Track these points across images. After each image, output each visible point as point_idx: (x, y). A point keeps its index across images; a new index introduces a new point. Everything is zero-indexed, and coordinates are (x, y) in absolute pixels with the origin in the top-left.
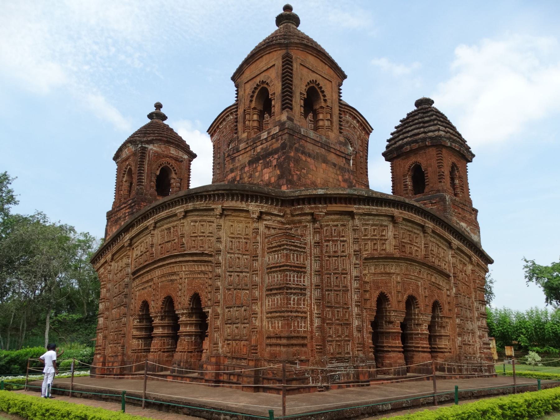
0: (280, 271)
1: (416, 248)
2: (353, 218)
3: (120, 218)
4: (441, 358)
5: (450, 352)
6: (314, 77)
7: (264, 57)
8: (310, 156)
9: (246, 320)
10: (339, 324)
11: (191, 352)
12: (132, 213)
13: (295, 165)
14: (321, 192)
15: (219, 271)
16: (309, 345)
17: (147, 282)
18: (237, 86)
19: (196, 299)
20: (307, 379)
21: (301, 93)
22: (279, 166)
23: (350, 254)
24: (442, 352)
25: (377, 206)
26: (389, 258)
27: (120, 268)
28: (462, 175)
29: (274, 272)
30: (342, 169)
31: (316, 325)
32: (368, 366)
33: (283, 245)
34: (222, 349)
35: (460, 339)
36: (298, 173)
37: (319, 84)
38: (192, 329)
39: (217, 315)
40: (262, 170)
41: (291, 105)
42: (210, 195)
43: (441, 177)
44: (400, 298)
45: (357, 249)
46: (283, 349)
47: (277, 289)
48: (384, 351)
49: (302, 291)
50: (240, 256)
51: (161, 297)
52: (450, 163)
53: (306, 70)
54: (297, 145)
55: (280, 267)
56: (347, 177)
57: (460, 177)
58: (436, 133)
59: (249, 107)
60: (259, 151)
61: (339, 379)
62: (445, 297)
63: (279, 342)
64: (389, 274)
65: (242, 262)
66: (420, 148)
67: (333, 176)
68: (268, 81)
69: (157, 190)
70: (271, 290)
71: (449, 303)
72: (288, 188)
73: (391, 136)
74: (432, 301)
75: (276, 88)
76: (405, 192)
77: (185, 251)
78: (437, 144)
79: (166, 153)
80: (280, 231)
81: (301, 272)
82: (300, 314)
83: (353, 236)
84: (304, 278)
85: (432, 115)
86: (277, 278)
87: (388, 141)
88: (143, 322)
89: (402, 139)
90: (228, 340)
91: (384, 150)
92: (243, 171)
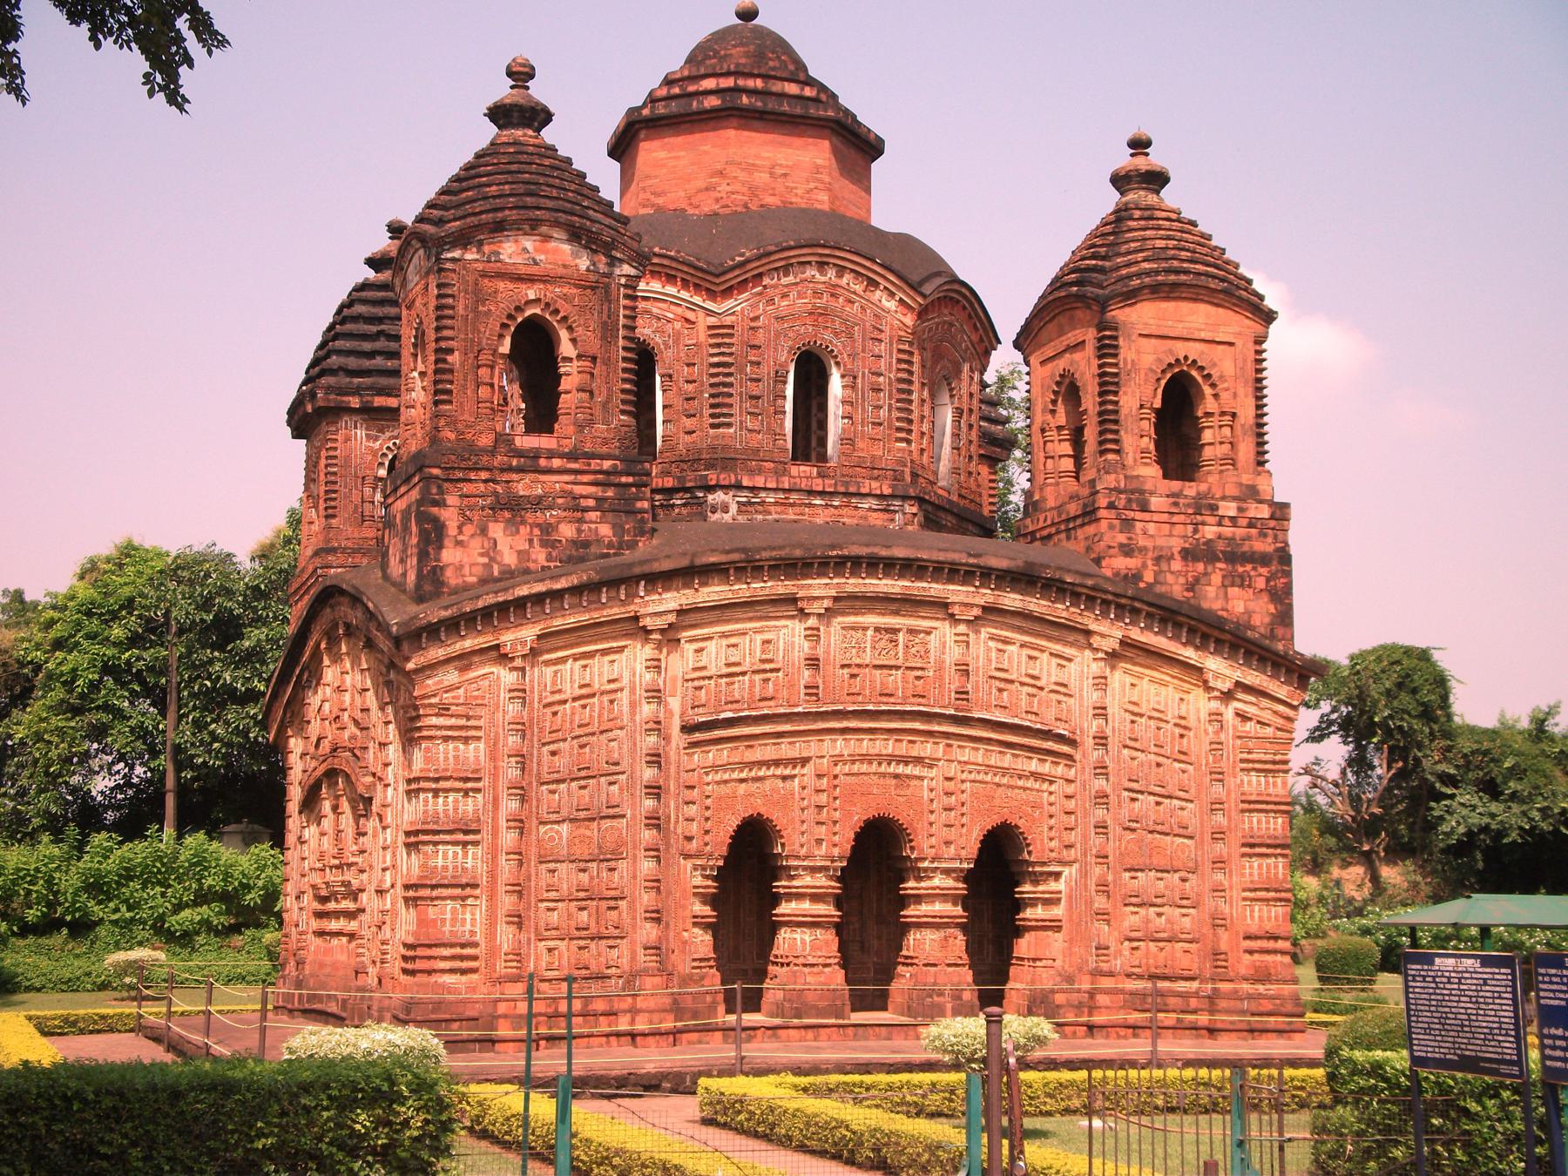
60: (1209, 536)
63: (1271, 945)
68: (1215, 373)
70: (1252, 846)
90: (1131, 940)
92: (1164, 567)
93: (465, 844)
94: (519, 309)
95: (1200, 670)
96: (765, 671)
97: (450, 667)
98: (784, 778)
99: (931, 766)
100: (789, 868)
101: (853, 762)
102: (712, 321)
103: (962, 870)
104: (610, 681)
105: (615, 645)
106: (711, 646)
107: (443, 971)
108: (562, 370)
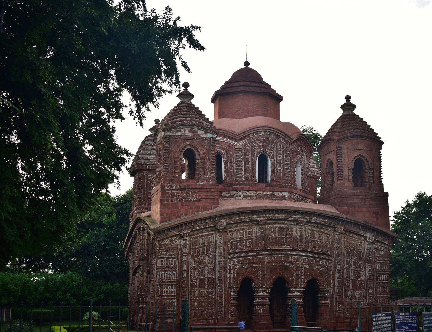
51: (271, 277)
93: (172, 285)
94: (185, 147)
95: (365, 237)
96: (249, 239)
97: (168, 240)
98: (255, 267)
99: (293, 263)
100: (256, 290)
101: (273, 263)
102: (236, 147)
103: (302, 291)
104: (209, 243)
105: (210, 233)
106: (235, 233)
107: (166, 318)
108: (196, 162)
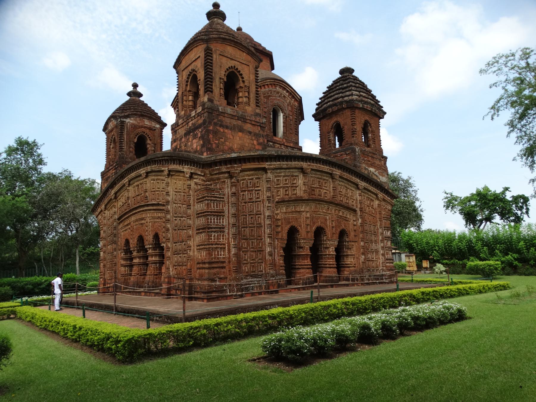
0: (204, 216)
1: (325, 191)
2: (266, 173)
3: (109, 177)
4: (347, 271)
5: (354, 267)
6: (232, 63)
7: (193, 50)
8: (227, 127)
9: (184, 251)
10: (253, 251)
11: (157, 275)
12: (116, 173)
13: (213, 136)
14: (234, 155)
15: (168, 217)
16: (227, 267)
17: (127, 225)
18: (177, 73)
19: (156, 236)
20: (225, 290)
21: (220, 78)
22: (202, 137)
23: (263, 200)
24: (348, 267)
25: (287, 161)
26: (299, 200)
27: (111, 215)
28: (374, 129)
29: (201, 216)
30: (257, 135)
31: (233, 253)
32: (283, 279)
33: (205, 197)
34: (172, 272)
35: (363, 257)
36: (217, 142)
37: (237, 69)
38: (157, 259)
39: (168, 248)
40: (192, 140)
41: (212, 88)
42: (160, 160)
43: (354, 132)
44: (309, 229)
45: (269, 195)
46: (207, 271)
47: (202, 229)
48: (296, 268)
49: (221, 229)
50: (181, 205)
52: (363, 121)
53: (225, 58)
54: (215, 121)
55: (204, 213)
56: (261, 141)
57: (372, 132)
58: (350, 97)
59: (186, 90)
61: (253, 289)
62: (351, 227)
64: (300, 212)
65: (182, 210)
66: (339, 110)
67: (248, 141)
68: (196, 70)
69: (135, 154)
71: (355, 231)
72: (207, 154)
73: (320, 101)
74: (339, 230)
75: (201, 75)
76: (329, 146)
77: (148, 202)
78: (351, 106)
79: (141, 124)
80: (203, 187)
81: (220, 216)
82: (219, 246)
83: (267, 186)
84: (223, 219)
85: (349, 82)
86: (201, 221)
87: (317, 104)
88: (127, 254)
89: (327, 103)
90: (176, 266)
91: (314, 112)
